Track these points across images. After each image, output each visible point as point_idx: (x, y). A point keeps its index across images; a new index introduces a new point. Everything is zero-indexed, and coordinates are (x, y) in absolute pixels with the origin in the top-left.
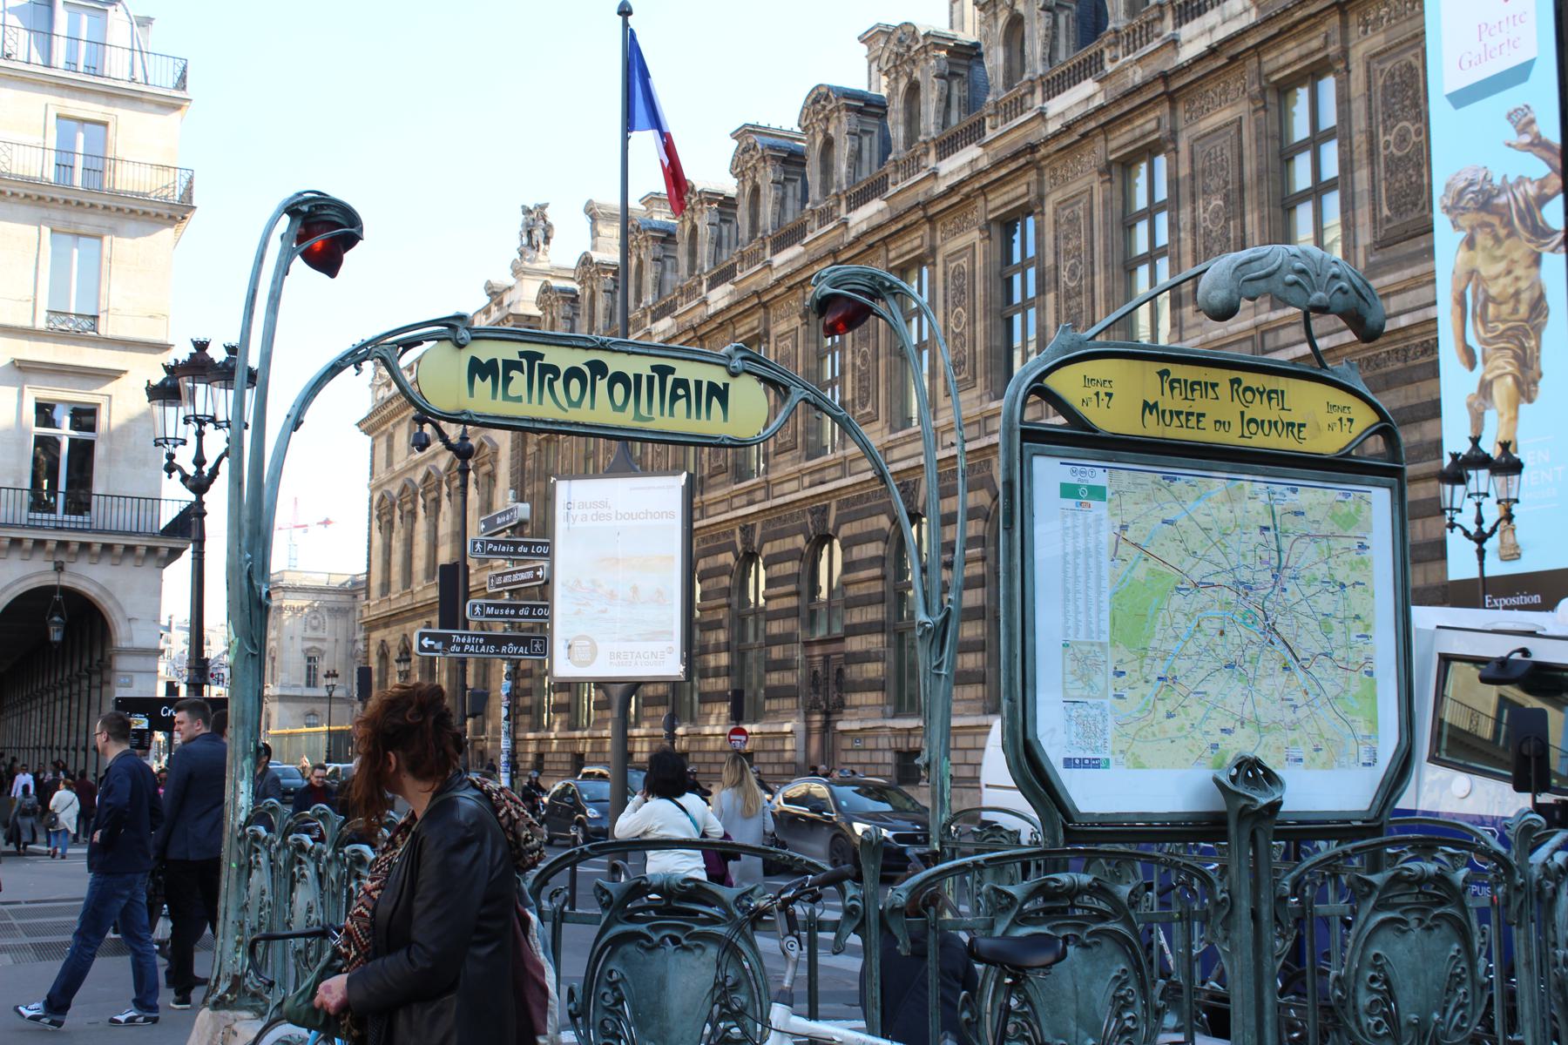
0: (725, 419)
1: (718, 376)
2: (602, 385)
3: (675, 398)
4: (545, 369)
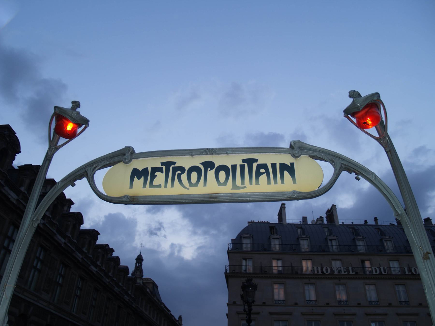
0: (294, 182)
1: (287, 159)
2: (211, 173)
3: (258, 174)
4: (175, 169)
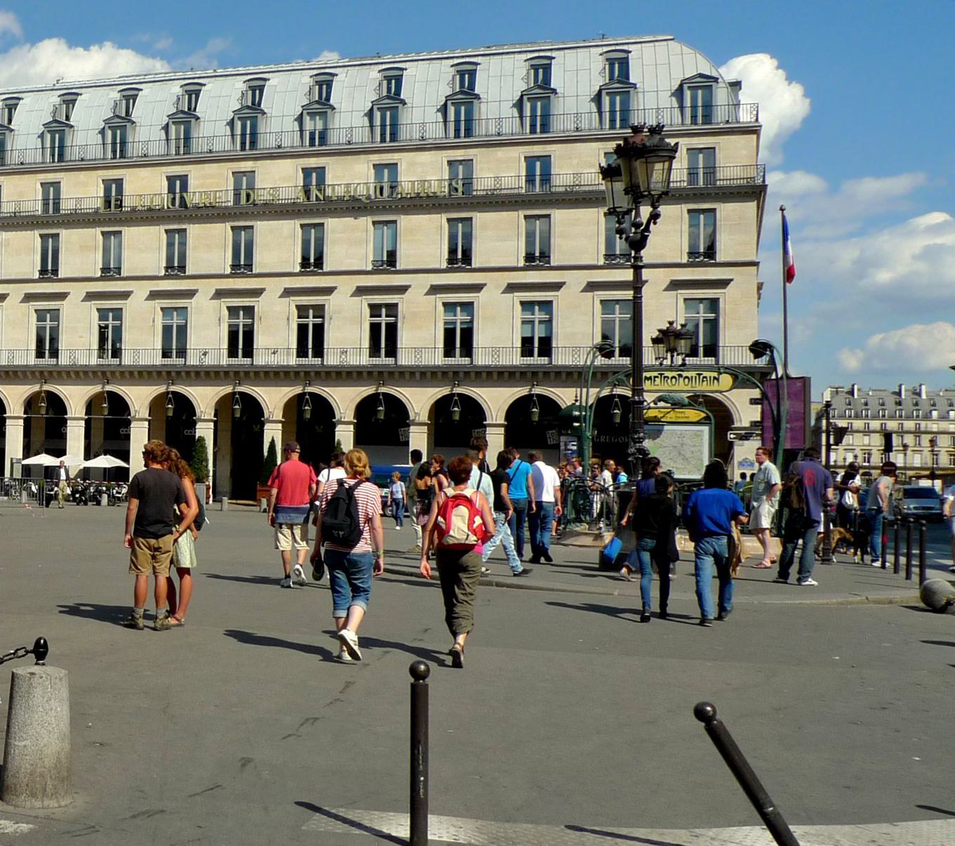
1: (715, 374)
3: (703, 381)
4: (665, 377)
